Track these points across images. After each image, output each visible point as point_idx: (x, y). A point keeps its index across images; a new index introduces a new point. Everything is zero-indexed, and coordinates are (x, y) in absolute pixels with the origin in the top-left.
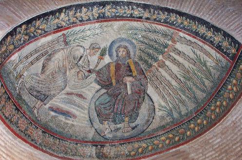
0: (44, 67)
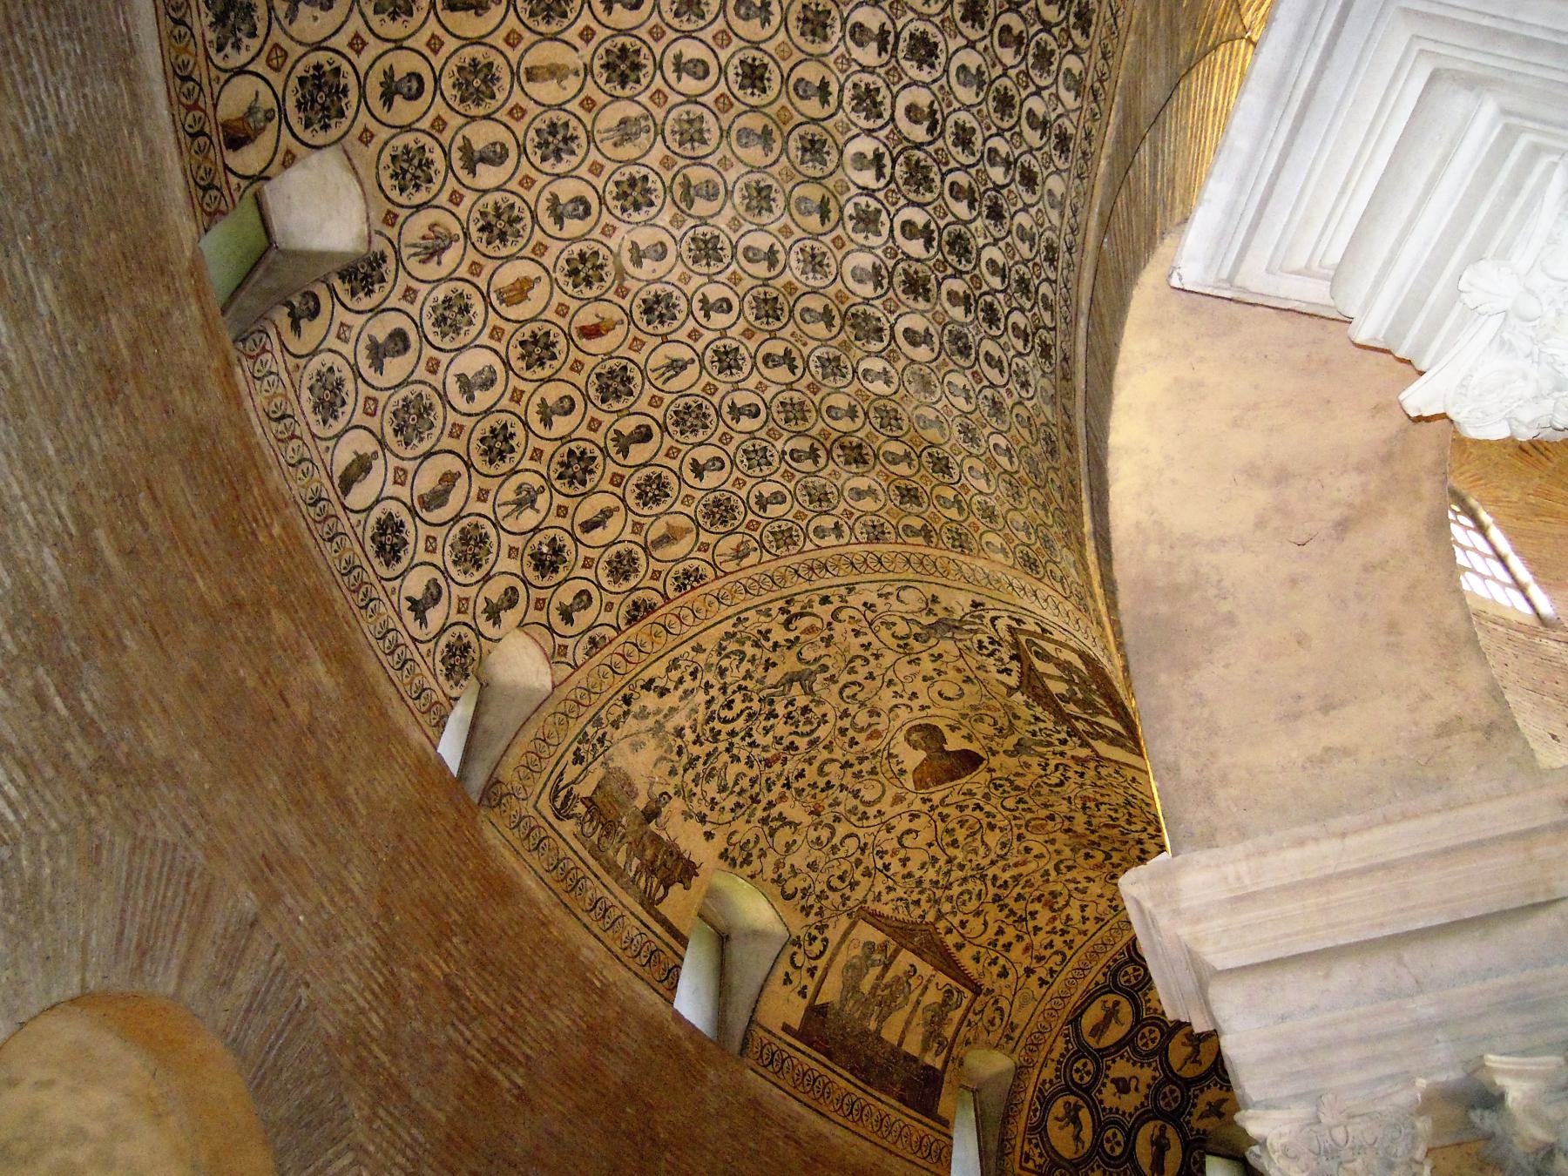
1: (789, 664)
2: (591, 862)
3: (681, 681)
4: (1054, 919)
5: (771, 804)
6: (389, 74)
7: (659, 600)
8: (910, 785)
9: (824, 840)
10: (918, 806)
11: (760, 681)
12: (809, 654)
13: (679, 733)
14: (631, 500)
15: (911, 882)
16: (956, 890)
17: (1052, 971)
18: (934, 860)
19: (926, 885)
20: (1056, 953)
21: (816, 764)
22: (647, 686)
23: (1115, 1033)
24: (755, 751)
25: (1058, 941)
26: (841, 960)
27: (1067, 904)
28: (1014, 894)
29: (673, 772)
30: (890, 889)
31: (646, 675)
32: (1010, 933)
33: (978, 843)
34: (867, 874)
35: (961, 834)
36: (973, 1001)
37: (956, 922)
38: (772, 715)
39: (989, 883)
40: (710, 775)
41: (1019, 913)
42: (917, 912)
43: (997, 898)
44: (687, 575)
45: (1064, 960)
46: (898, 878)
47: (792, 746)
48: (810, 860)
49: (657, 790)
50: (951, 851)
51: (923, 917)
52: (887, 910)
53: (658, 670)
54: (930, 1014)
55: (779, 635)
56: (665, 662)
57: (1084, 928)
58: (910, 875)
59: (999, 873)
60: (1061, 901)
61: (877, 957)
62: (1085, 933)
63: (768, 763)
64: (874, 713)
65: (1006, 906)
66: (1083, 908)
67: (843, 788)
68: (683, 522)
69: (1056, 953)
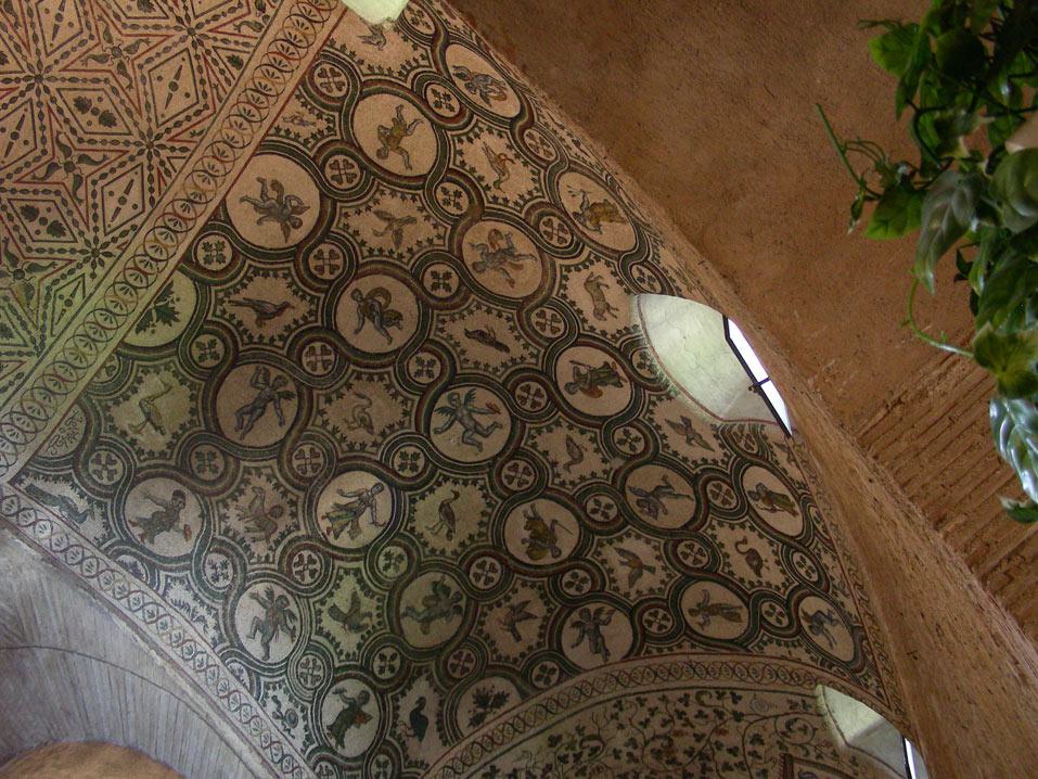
4: (677, 734)
17: (720, 696)
23: (719, 594)
25: (692, 711)
27: (659, 737)
32: (723, 756)
36: (800, 761)
57: (658, 703)
60: (657, 744)
62: (664, 699)
66: (645, 724)
69: (702, 704)
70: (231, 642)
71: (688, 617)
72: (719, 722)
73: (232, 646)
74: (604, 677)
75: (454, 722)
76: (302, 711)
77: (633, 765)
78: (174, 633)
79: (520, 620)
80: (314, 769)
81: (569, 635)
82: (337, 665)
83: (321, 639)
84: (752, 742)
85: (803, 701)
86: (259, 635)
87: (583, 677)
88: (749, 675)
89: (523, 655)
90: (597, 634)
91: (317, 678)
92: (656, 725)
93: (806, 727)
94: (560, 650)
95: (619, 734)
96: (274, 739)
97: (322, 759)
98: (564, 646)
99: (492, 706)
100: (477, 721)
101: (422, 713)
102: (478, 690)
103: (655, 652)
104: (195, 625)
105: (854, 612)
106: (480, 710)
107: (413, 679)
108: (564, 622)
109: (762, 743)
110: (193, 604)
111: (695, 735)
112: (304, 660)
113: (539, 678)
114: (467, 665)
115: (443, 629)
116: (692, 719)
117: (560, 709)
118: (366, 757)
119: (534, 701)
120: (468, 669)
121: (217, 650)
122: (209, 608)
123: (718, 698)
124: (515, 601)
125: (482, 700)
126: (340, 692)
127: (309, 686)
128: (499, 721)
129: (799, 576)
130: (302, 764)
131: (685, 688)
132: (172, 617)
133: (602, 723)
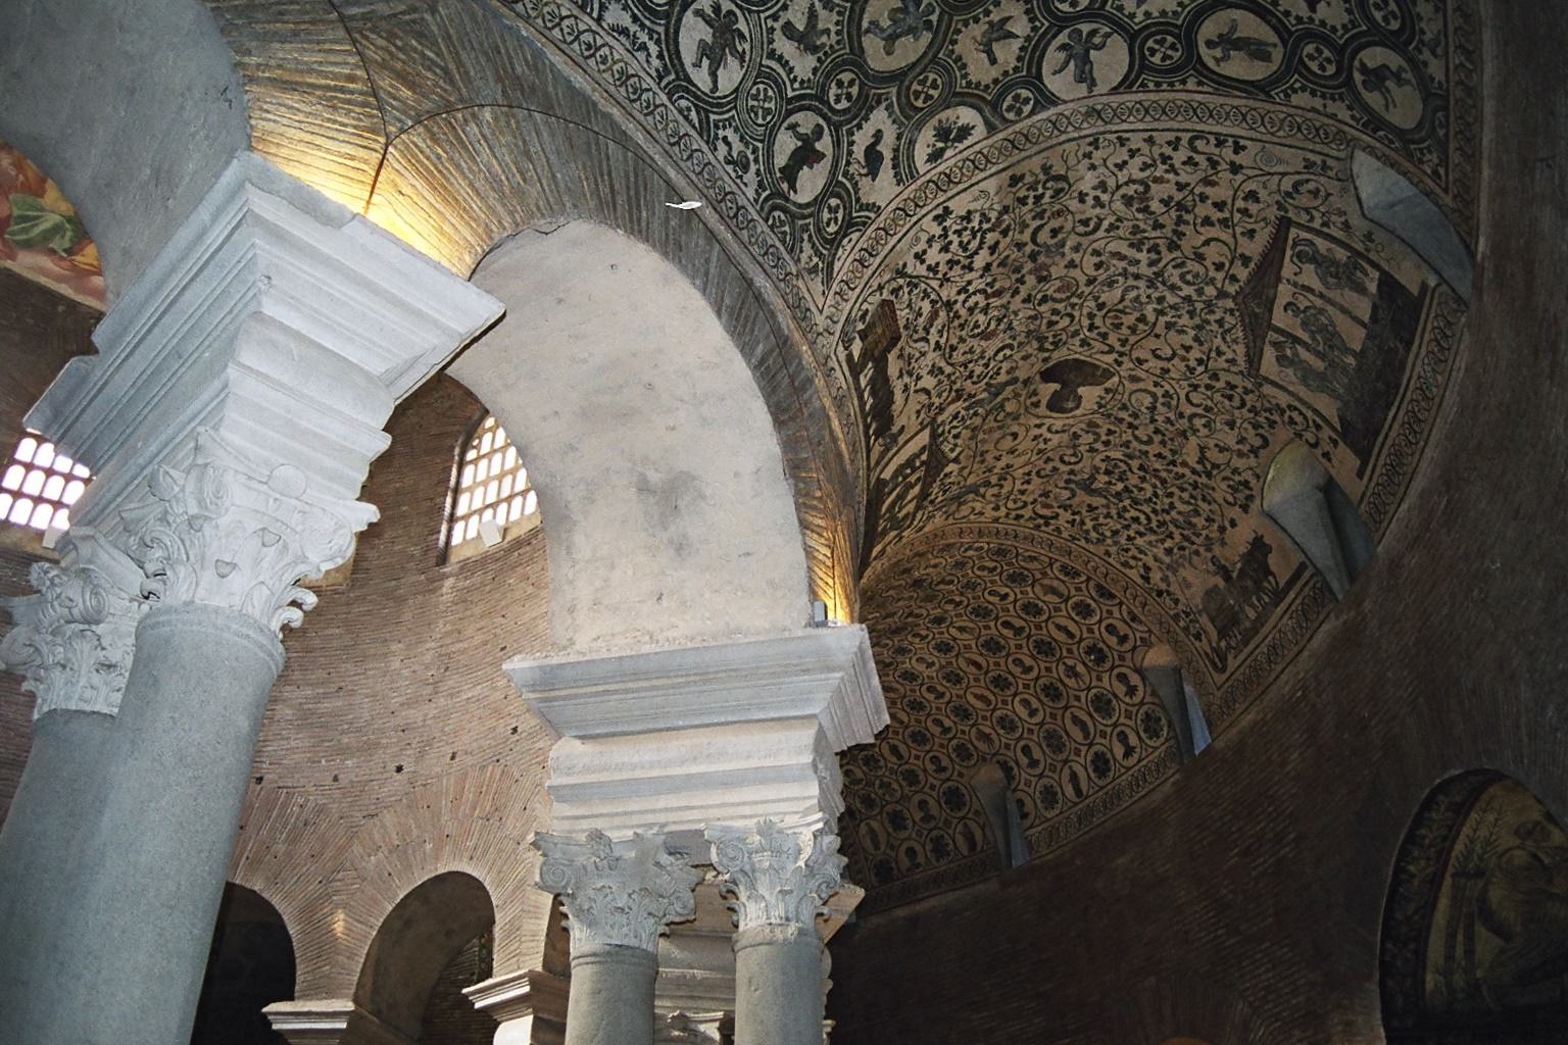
0: (1498, 930)
1: (1082, 497)
2: (1288, 600)
3: (1134, 558)
4: (1157, 180)
5: (1194, 472)
6: (936, 771)
7: (1092, 584)
8: (1116, 379)
9: (1203, 421)
10: (1127, 364)
11: (1108, 507)
12: (1066, 494)
13: (1169, 551)
14: (1045, 617)
15: (1203, 336)
16: (1188, 290)
17: (1220, 144)
18: (1169, 326)
19: (1197, 321)
20: (1194, 150)
21: (1144, 448)
22: (1147, 579)
23: (1249, 25)
24: (1160, 492)
26: (1302, 392)
27: (1131, 181)
28: (1158, 233)
29: (1197, 553)
30: (1220, 353)
31: (1140, 581)
33: (1125, 303)
34: (1215, 377)
35: (1129, 320)
36: (1300, 226)
37: (1220, 276)
38: (1126, 489)
39: (1161, 265)
40: (1190, 523)
41: (1174, 214)
42: (1230, 320)
43: (1173, 246)
44: (1067, 574)
45: (1199, 135)
46: (1205, 347)
47: (1141, 467)
48: (1226, 428)
49: (1212, 568)
50: (1151, 318)
51: (1231, 311)
52: (1241, 349)
53: (1133, 574)
54: (1331, 280)
55: (1067, 516)
56: (1127, 571)
57: (1141, 144)
58: (1196, 339)
59: (1144, 262)
60: (1130, 190)
61: (1289, 352)
62: (1150, 141)
63: (1164, 482)
64: (1076, 436)
65: (1175, 232)
66: (1121, 166)
67: (1153, 421)
68: (1038, 588)
69: (1194, 150)
70: (677, 73)
71: (1203, 50)
72: (1211, 172)
73: (678, 78)
74: (1083, 110)
75: (911, 157)
76: (753, 152)
77: (1098, 210)
78: (615, 67)
79: (997, 40)
80: (767, 221)
81: (1053, 57)
82: (790, 94)
83: (773, 64)
84: (1245, 199)
85: (1324, 162)
86: (706, 62)
87: (1060, 108)
88: (1263, 124)
89: (996, 81)
90: (1085, 60)
91: (767, 111)
92: (1134, 170)
93: (1318, 190)
94: (1039, 77)
95: (1089, 175)
96: (728, 189)
97: (774, 208)
98: (1044, 71)
99: (954, 140)
100: (935, 156)
101: (878, 148)
102: (940, 121)
103: (1151, 86)
104: (637, 54)
105: (1439, 76)
106: (940, 145)
107: (871, 109)
108: (1049, 43)
109: (1257, 200)
110: (633, 28)
111: (1177, 183)
112: (754, 91)
113: (1009, 109)
114: (931, 92)
115: (910, 50)
116: (1177, 165)
117: (1028, 145)
118: (819, 201)
119: (1001, 136)
120: (932, 97)
121: (663, 84)
122: (651, 32)
123: (1216, 146)
124: (995, 17)
125: (943, 134)
126: (793, 127)
127: (760, 121)
128: (959, 157)
129: (1370, 19)
130: (756, 217)
131: (1178, 130)
132: (611, 47)
133: (1072, 161)
